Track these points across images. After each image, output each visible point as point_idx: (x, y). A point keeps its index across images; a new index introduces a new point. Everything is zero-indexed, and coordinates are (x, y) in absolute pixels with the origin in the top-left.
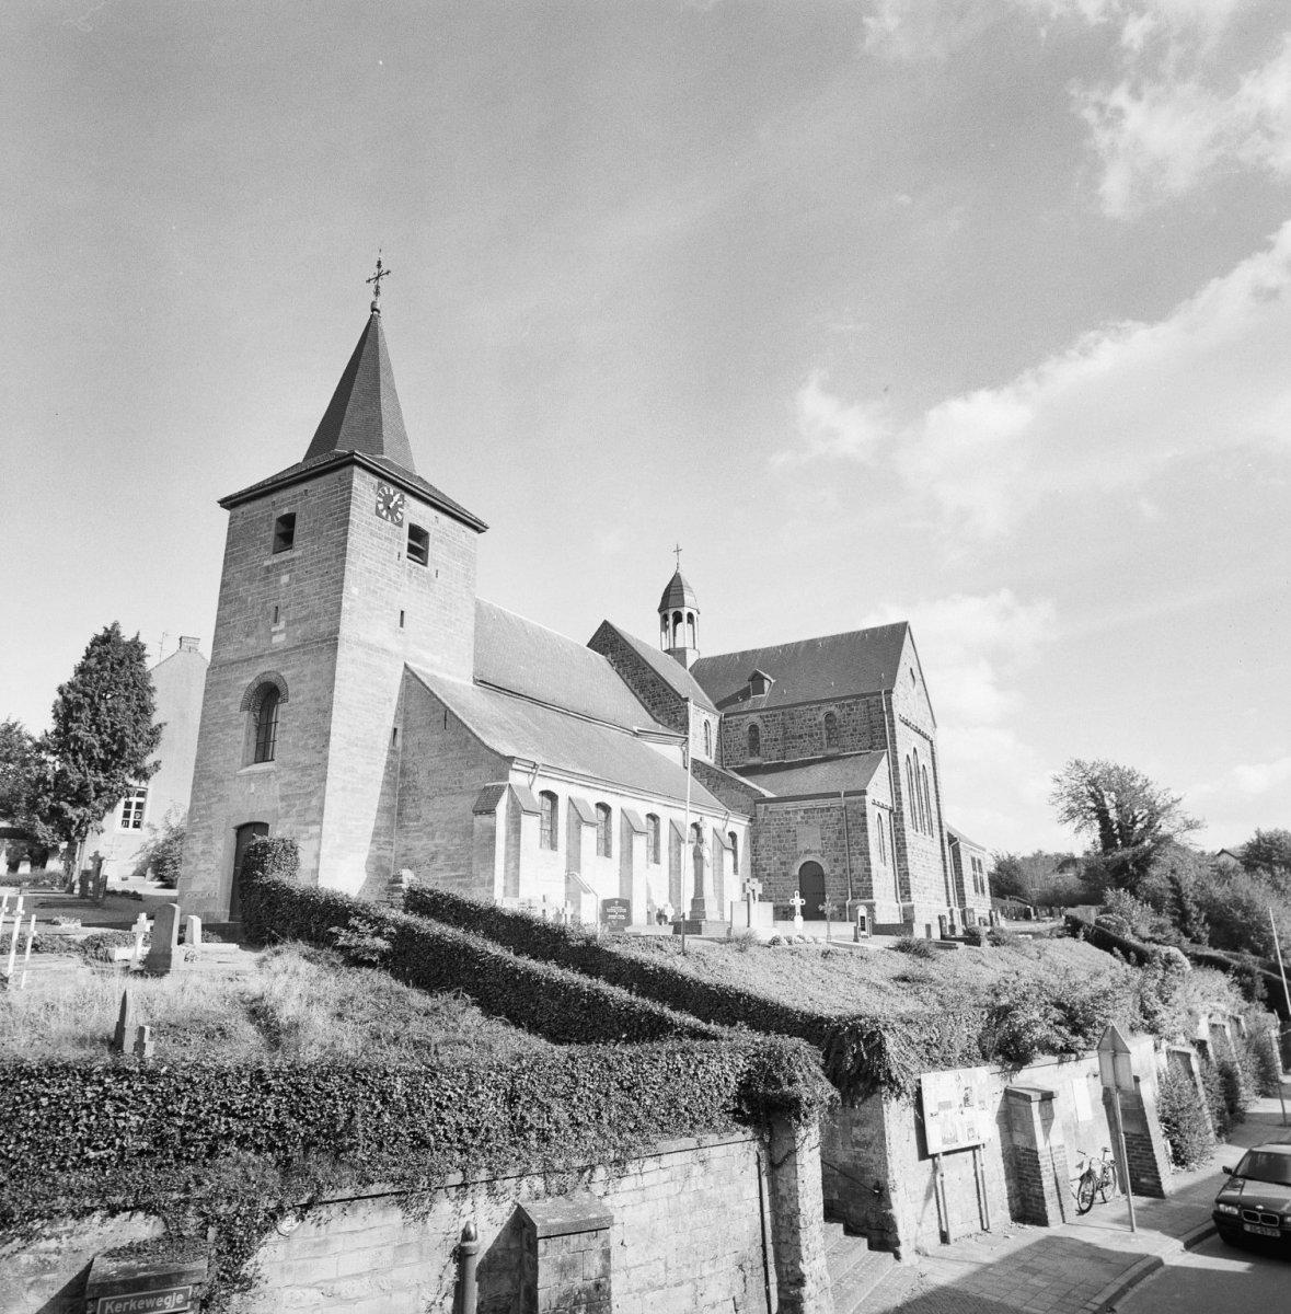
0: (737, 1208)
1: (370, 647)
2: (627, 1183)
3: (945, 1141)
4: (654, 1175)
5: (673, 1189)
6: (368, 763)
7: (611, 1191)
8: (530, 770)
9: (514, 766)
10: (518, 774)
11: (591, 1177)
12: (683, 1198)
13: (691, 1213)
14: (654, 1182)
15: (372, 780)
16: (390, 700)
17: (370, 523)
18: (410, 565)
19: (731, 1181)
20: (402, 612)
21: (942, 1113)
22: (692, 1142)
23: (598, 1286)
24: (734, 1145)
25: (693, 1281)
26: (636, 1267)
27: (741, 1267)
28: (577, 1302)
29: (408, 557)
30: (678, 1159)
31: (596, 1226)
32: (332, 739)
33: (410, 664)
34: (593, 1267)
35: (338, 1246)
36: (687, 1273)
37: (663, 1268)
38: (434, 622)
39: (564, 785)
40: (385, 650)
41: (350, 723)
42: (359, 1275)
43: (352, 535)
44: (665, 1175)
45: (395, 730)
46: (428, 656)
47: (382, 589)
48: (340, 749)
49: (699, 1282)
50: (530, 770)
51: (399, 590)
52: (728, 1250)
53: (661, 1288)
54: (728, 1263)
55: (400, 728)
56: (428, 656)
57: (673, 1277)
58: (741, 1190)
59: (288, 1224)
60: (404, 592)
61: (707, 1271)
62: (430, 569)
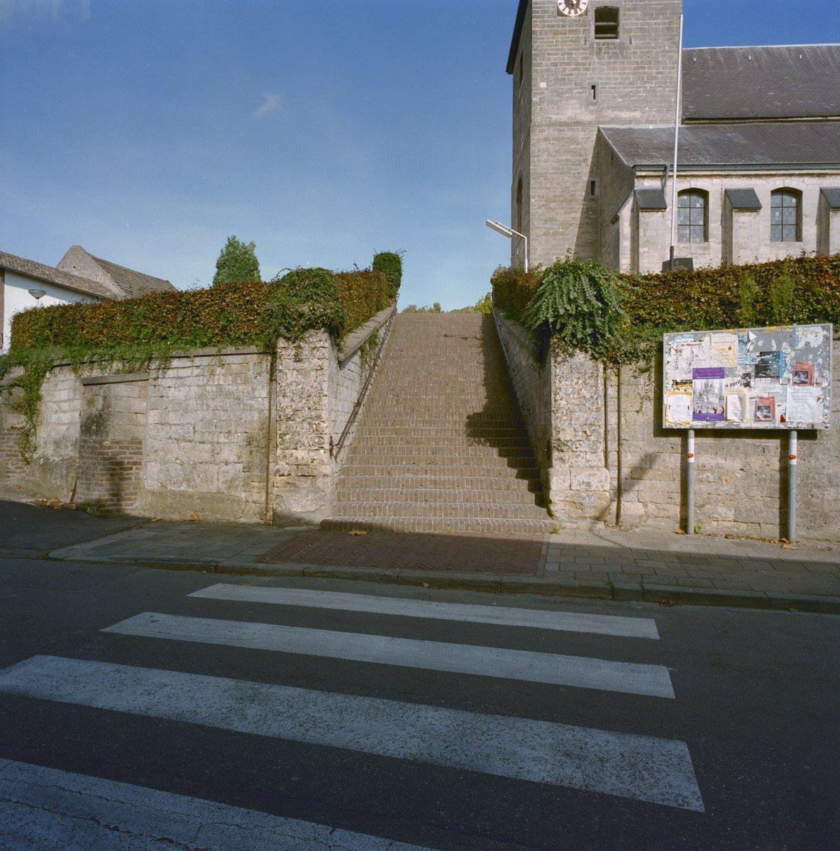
0: (249, 402)
1: (562, 124)
2: (170, 373)
3: (697, 416)
4: (190, 370)
5: (201, 381)
6: (566, 213)
7: (160, 376)
8: (661, 173)
9: (638, 174)
10: (641, 180)
11: (149, 366)
12: (208, 388)
13: (213, 399)
14: (190, 375)
15: (571, 224)
16: (585, 160)
17: (553, 26)
18: (598, 44)
19: (246, 382)
20: (593, 87)
21: (699, 384)
22: (213, 350)
23: (101, 415)
24: (250, 356)
25: (212, 443)
26: (175, 425)
27: (249, 444)
28: (93, 422)
29: (596, 38)
30: (206, 361)
31: (100, 381)
32: (532, 200)
33: (600, 126)
34: (99, 404)
35: (59, 387)
36: (207, 437)
37: (192, 430)
38: (630, 83)
39: (716, 181)
40: (578, 123)
41: (548, 186)
42: (65, 401)
43: (535, 42)
44: (196, 371)
45: (593, 183)
46: (625, 115)
47: (571, 75)
48: (539, 207)
49: (216, 445)
50: (661, 173)
51: (587, 69)
52: (240, 430)
53: (190, 441)
54: (240, 438)
55: (597, 180)
56: (625, 115)
57: (198, 437)
58: (254, 390)
59: (48, 375)
60: (594, 69)
61: (222, 439)
62: (623, 36)
